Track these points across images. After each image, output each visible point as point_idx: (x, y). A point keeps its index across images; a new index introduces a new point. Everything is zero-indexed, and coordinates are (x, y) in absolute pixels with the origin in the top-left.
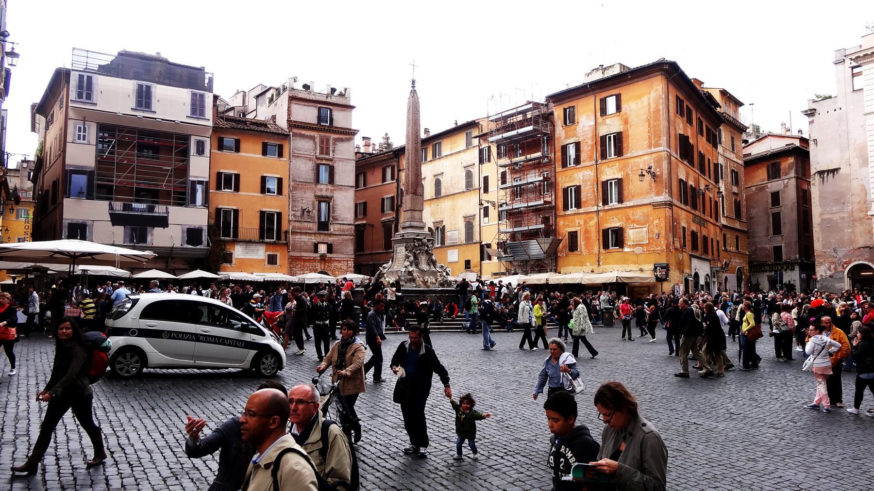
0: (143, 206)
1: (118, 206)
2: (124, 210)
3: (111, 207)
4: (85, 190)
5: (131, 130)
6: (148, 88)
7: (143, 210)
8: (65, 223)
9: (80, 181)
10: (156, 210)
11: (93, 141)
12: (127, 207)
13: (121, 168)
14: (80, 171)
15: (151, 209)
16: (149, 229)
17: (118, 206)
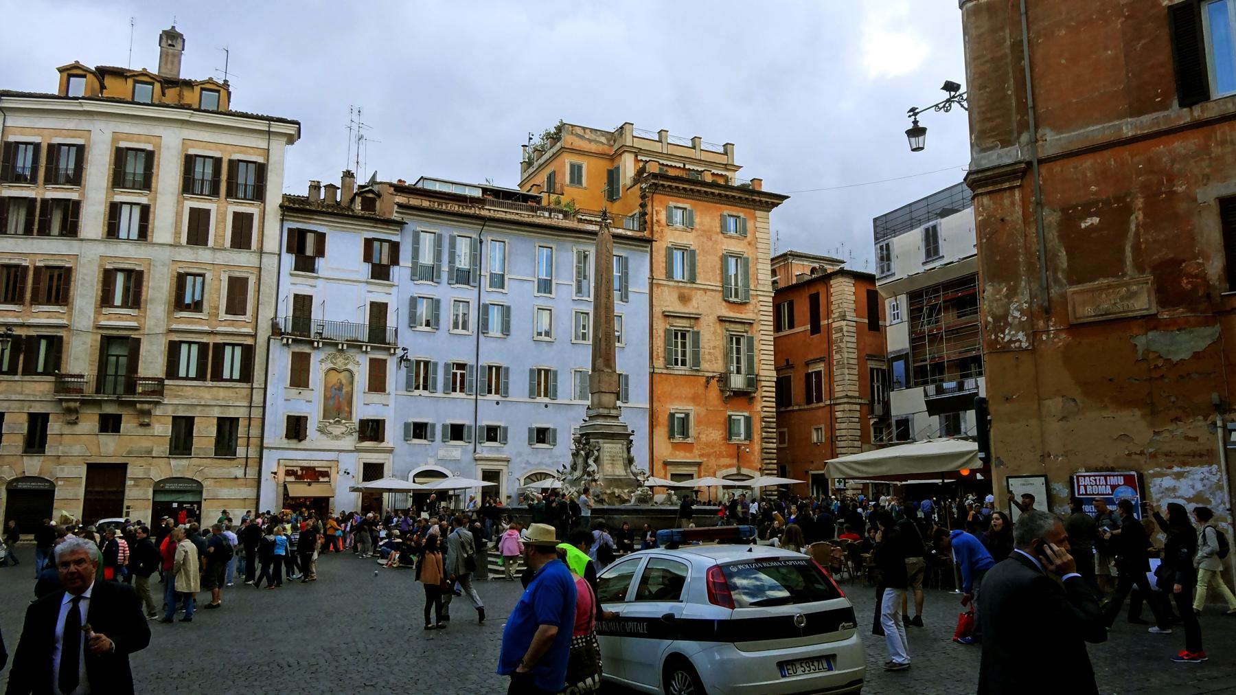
0: (953, 384)
1: (931, 389)
2: (937, 394)
3: (926, 395)
4: (903, 380)
5: (935, 289)
6: (934, 227)
7: (953, 390)
8: (894, 423)
9: (899, 366)
10: (966, 387)
11: (905, 318)
12: (940, 390)
13: (935, 339)
14: (898, 358)
15: (961, 387)
16: (961, 414)
17: (931, 389)
